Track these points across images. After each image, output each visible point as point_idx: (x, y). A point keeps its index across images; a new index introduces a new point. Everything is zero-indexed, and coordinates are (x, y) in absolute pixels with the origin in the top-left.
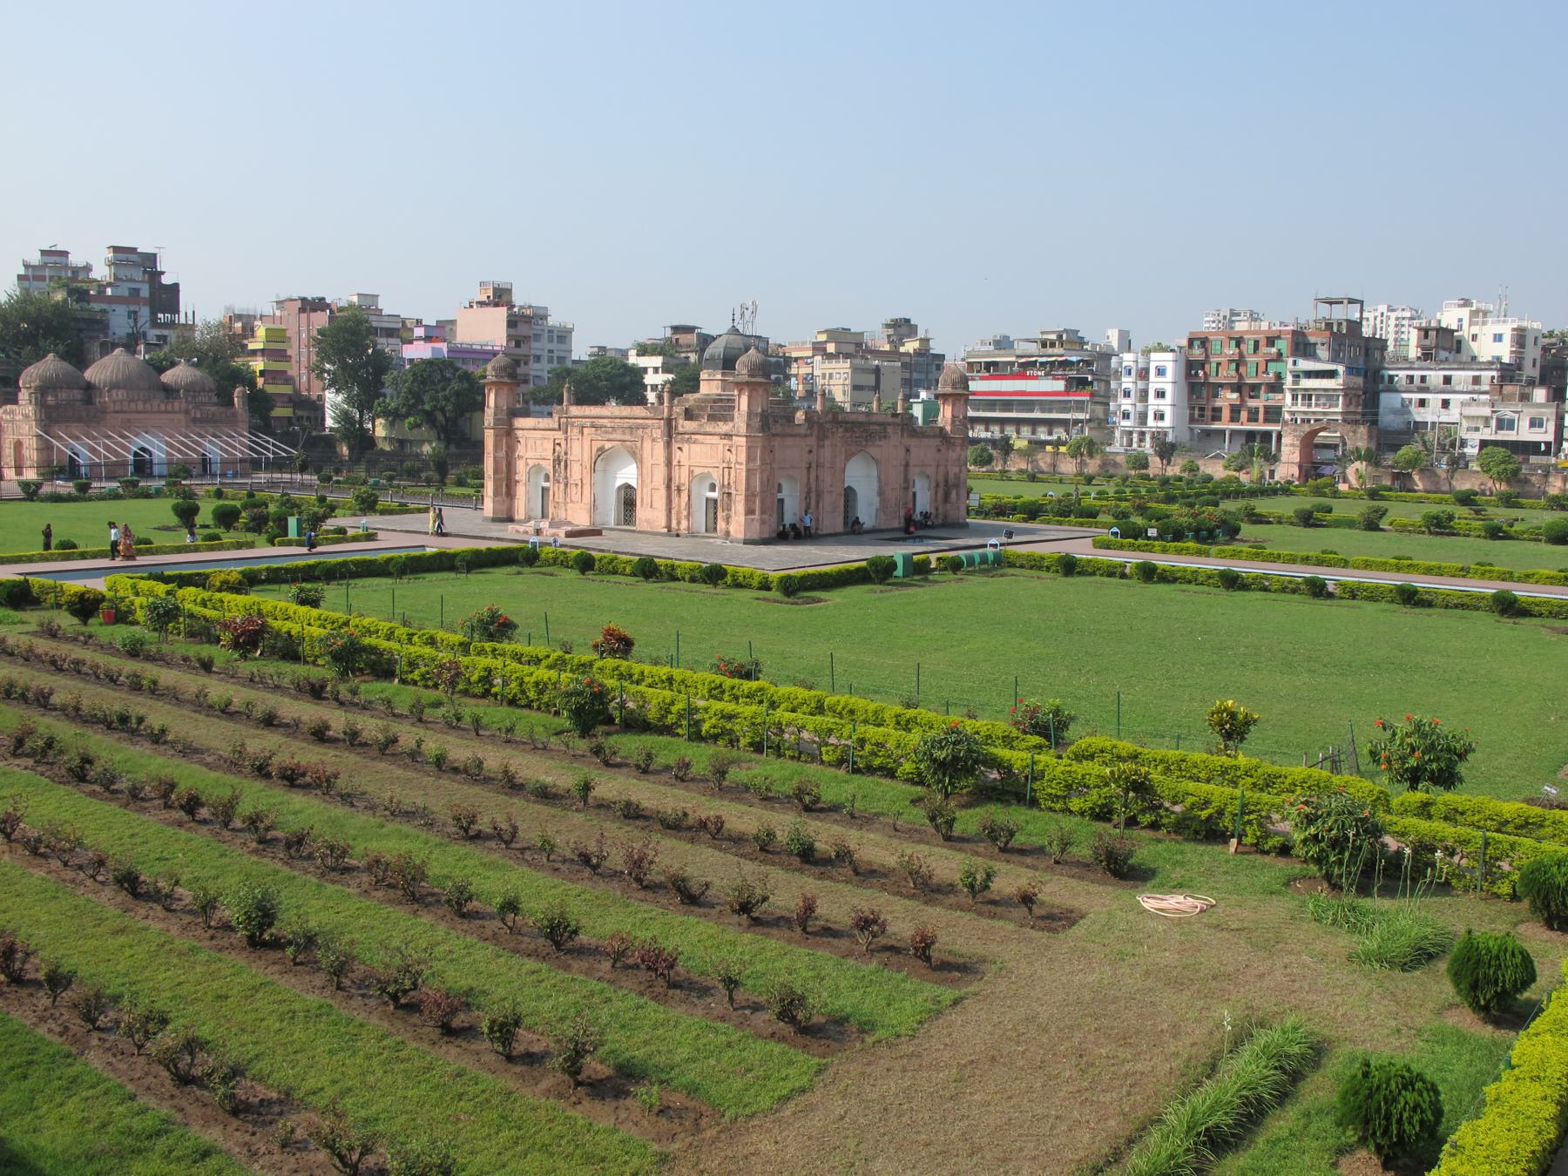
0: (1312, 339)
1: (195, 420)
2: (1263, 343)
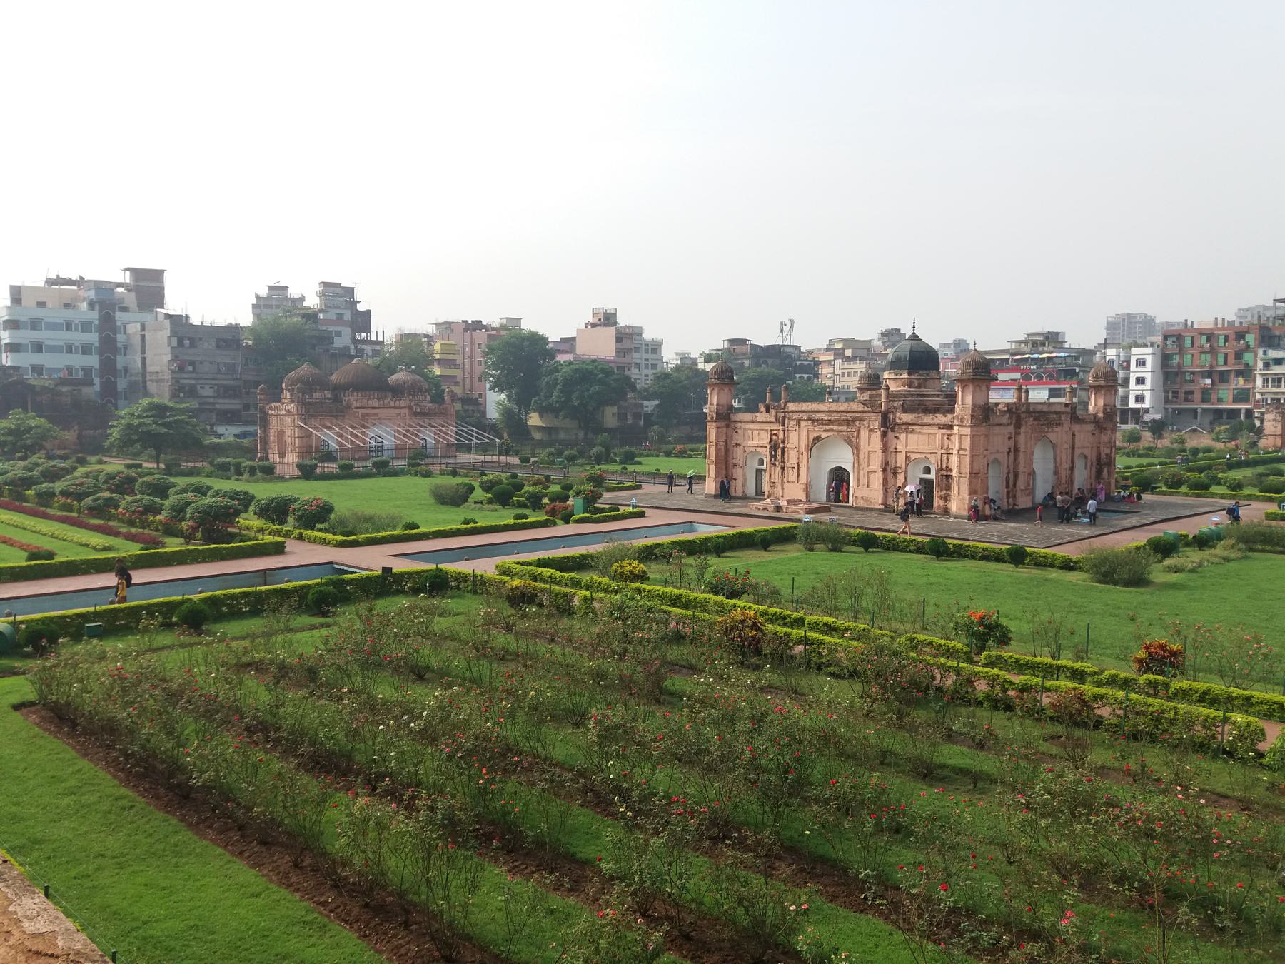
0: (1277, 333)
1: (416, 414)
2: (1232, 337)
